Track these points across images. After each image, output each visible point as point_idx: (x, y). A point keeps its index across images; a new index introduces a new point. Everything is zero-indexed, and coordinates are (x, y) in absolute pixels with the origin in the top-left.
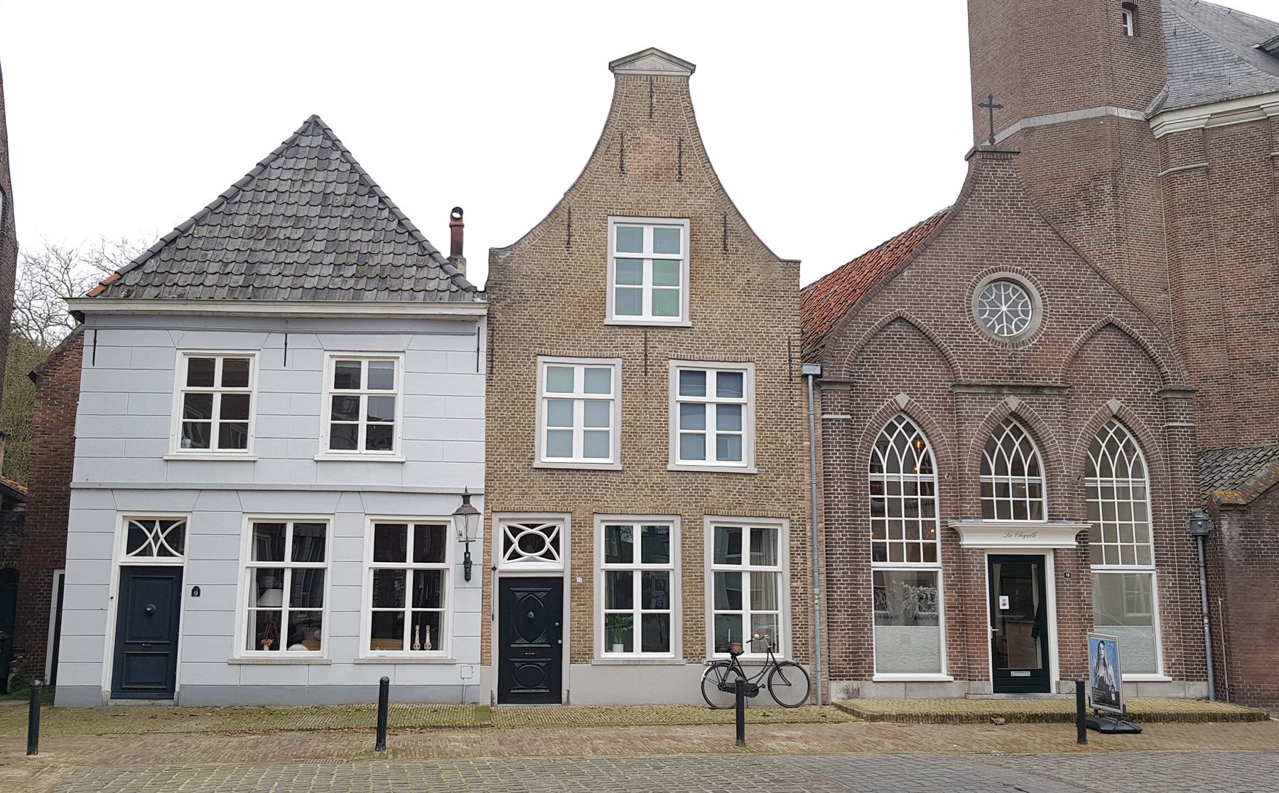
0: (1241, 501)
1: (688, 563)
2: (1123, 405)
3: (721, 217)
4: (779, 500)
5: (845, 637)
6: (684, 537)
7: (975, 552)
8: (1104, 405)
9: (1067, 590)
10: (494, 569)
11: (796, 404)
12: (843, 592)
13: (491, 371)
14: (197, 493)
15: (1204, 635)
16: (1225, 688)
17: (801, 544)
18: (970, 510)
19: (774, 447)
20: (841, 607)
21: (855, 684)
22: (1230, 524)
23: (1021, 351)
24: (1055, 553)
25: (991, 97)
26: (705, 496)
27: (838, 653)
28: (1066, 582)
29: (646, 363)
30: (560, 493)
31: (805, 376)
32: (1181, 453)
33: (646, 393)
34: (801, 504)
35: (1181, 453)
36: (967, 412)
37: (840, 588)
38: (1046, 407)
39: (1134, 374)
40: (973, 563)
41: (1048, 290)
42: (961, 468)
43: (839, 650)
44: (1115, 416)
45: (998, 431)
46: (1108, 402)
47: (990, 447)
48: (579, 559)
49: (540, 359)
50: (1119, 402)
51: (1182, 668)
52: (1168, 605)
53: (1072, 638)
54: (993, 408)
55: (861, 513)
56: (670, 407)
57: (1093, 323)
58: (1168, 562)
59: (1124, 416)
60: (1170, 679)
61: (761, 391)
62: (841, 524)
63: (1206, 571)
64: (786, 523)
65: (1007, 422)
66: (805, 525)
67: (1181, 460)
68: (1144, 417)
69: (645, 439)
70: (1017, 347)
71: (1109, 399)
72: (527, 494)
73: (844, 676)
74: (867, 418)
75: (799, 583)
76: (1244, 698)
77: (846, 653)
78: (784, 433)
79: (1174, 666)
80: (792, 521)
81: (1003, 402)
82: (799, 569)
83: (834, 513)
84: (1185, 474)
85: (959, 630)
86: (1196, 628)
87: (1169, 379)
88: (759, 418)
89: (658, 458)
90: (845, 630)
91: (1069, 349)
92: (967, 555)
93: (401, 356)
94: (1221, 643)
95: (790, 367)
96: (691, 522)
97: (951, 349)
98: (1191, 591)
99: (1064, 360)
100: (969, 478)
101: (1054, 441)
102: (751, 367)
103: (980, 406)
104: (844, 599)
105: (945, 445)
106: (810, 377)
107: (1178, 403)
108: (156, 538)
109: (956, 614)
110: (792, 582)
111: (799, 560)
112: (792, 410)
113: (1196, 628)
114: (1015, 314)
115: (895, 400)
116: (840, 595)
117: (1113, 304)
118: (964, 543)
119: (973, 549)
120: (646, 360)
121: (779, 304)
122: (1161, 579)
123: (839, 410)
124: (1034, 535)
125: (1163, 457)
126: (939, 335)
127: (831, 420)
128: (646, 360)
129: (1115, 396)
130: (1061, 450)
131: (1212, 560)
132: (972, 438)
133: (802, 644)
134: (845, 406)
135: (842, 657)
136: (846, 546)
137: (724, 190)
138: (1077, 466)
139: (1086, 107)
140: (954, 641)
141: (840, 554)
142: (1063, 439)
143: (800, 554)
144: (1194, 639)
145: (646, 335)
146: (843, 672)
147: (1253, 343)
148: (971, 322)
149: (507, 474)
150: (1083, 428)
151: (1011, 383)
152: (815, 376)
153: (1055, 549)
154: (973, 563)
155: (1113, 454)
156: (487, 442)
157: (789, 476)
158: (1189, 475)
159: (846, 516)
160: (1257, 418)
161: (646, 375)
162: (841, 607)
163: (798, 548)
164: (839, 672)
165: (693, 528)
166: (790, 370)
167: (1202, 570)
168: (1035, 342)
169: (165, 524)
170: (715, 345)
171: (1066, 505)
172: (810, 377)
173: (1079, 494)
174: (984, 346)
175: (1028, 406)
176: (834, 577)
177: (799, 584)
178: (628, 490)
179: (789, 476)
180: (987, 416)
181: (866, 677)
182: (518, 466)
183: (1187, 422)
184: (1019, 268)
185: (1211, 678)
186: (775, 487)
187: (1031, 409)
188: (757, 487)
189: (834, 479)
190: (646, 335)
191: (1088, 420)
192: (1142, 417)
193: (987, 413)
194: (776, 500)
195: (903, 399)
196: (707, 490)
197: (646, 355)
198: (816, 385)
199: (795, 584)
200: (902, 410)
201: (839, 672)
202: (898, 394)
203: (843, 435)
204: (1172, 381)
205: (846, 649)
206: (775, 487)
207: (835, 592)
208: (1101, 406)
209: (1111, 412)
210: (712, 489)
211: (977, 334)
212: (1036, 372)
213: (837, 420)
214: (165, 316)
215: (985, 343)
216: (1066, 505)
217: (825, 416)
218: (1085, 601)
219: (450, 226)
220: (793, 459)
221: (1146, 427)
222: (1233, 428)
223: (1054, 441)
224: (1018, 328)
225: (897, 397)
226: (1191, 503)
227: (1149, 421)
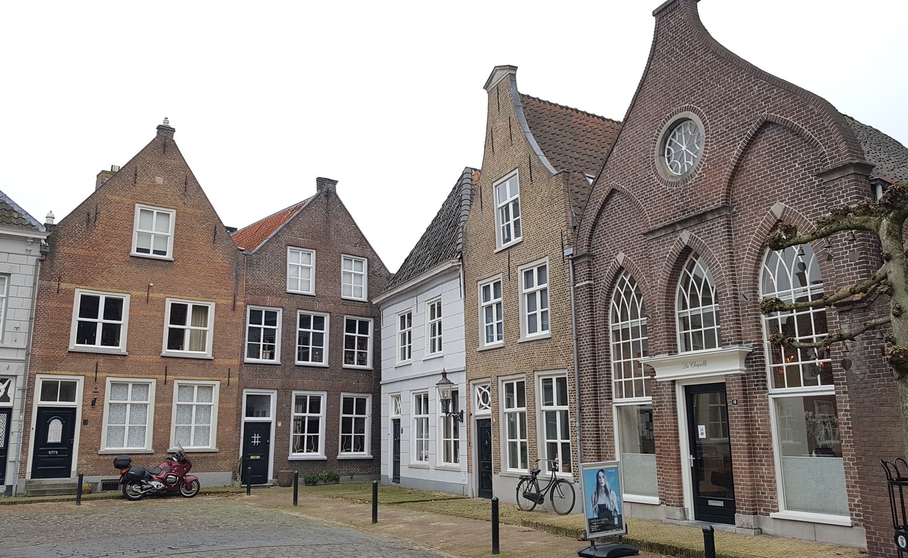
2: (787, 206)
7: (664, 385)
8: (769, 212)
14: (428, 378)
18: (660, 346)
23: (690, 185)
28: (735, 410)
35: (842, 245)
38: (710, 233)
39: (797, 166)
40: (663, 395)
41: (709, 115)
50: (783, 204)
53: (742, 468)
54: (672, 247)
57: (748, 129)
68: (809, 213)
70: (687, 182)
71: (772, 204)
79: (857, 509)
84: (848, 270)
87: (826, 160)
91: (727, 167)
99: (723, 180)
103: (663, 248)
117: (767, 100)
119: (663, 382)
126: (635, 194)
129: (779, 199)
130: (724, 272)
132: (658, 279)
138: (746, 285)
142: (726, 261)
150: (750, 244)
151: (684, 217)
154: (663, 395)
158: (852, 269)
168: (700, 171)
171: (731, 328)
173: (749, 315)
174: (664, 190)
175: (696, 236)
184: (687, 105)
187: (700, 238)
191: (753, 233)
192: (807, 213)
195: (621, 257)
202: (618, 254)
204: (829, 161)
207: (585, 425)
208: (765, 214)
209: (775, 217)
212: (702, 201)
215: (664, 188)
218: (759, 429)
221: (811, 223)
223: (719, 265)
225: (618, 257)
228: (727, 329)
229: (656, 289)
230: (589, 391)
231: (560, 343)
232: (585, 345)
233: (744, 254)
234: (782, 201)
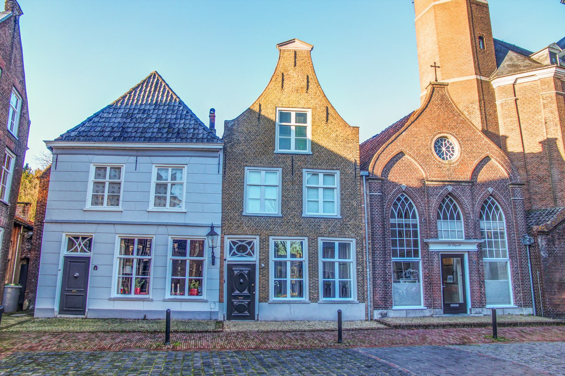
0: (546, 230)
1: (311, 258)
3: (325, 109)
4: (351, 230)
5: (380, 290)
6: (309, 246)
9: (474, 269)
10: (225, 260)
11: (358, 188)
12: (380, 270)
13: (224, 173)
15: (530, 288)
16: (541, 310)
19: (349, 207)
20: (379, 277)
21: (385, 311)
22: (541, 240)
23: (452, 167)
24: (468, 253)
25: (435, 63)
26: (319, 228)
27: (378, 297)
28: (474, 265)
29: (292, 170)
30: (254, 227)
31: (362, 176)
32: (518, 210)
33: (292, 183)
34: (361, 232)
35: (518, 210)
36: (431, 192)
37: (378, 269)
40: (435, 257)
42: (429, 216)
43: (378, 297)
44: (491, 195)
45: (443, 201)
46: (488, 189)
47: (440, 208)
48: (263, 256)
49: (246, 168)
51: (522, 302)
52: (515, 275)
53: (477, 289)
55: (387, 236)
56: (303, 189)
57: (481, 155)
58: (514, 256)
59: (494, 195)
60: (517, 307)
61: (343, 182)
62: (378, 241)
63: (531, 260)
64: (354, 240)
65: (447, 197)
66: (362, 241)
67: (519, 213)
69: (292, 203)
72: (240, 227)
73: (380, 308)
76: (550, 315)
80: (357, 239)
81: (445, 188)
82: (360, 260)
83: (376, 236)
84: (520, 219)
85: (429, 287)
86: (527, 285)
88: (342, 194)
89: (298, 212)
90: (380, 287)
92: (432, 254)
93: (186, 166)
94: (539, 291)
95: (355, 172)
97: (424, 165)
98: (524, 269)
100: (433, 221)
101: (467, 205)
102: (338, 172)
104: (380, 274)
105: (422, 206)
106: (364, 176)
107: (516, 189)
108: (80, 245)
109: (428, 280)
110: (357, 266)
111: (360, 257)
112: (356, 191)
113: (527, 285)
114: (449, 151)
115: (400, 187)
116: (378, 272)
118: (431, 249)
120: (292, 168)
121: (350, 145)
122: (512, 264)
123: (377, 191)
125: (511, 212)
127: (374, 195)
128: (292, 168)
131: (533, 255)
133: (362, 294)
134: (379, 189)
135: (379, 299)
136: (381, 250)
139: (466, 75)
140: (427, 291)
141: (378, 254)
143: (360, 254)
144: (526, 289)
145: (292, 158)
147: (537, 168)
148: (432, 154)
149: (231, 218)
152: (366, 176)
153: (468, 251)
154: (435, 257)
155: (490, 211)
156: (222, 204)
157: (355, 220)
159: (381, 237)
160: (540, 199)
161: (292, 175)
162: (379, 277)
163: (360, 251)
164: (378, 306)
165: (313, 242)
166: (355, 174)
167: (529, 260)
168: (458, 163)
169: (84, 238)
170: (322, 162)
171: (473, 232)
172: (364, 176)
176: (376, 264)
177: (360, 267)
178: (284, 225)
179: (355, 220)
180: (439, 194)
181: (390, 308)
182: (236, 215)
183: (520, 197)
184: (450, 132)
186: (349, 225)
188: (341, 224)
189: (375, 221)
190: (292, 158)
192: (502, 195)
193: (439, 193)
194: (350, 230)
196: (320, 226)
197: (292, 167)
199: (358, 267)
200: (403, 192)
201: (378, 306)
203: (379, 202)
205: (381, 296)
206: (349, 225)
207: (376, 271)
208: (485, 190)
211: (434, 159)
213: (376, 195)
214: (84, 149)
216: (473, 232)
217: (371, 194)
219: (210, 116)
220: (357, 212)
221: (504, 199)
222: (530, 203)
223: (467, 205)
224: (450, 157)
226: (523, 232)
227: (505, 197)
228: (471, 232)
229: (432, 208)
231: (349, 223)
233: (476, 203)
234: (492, 188)
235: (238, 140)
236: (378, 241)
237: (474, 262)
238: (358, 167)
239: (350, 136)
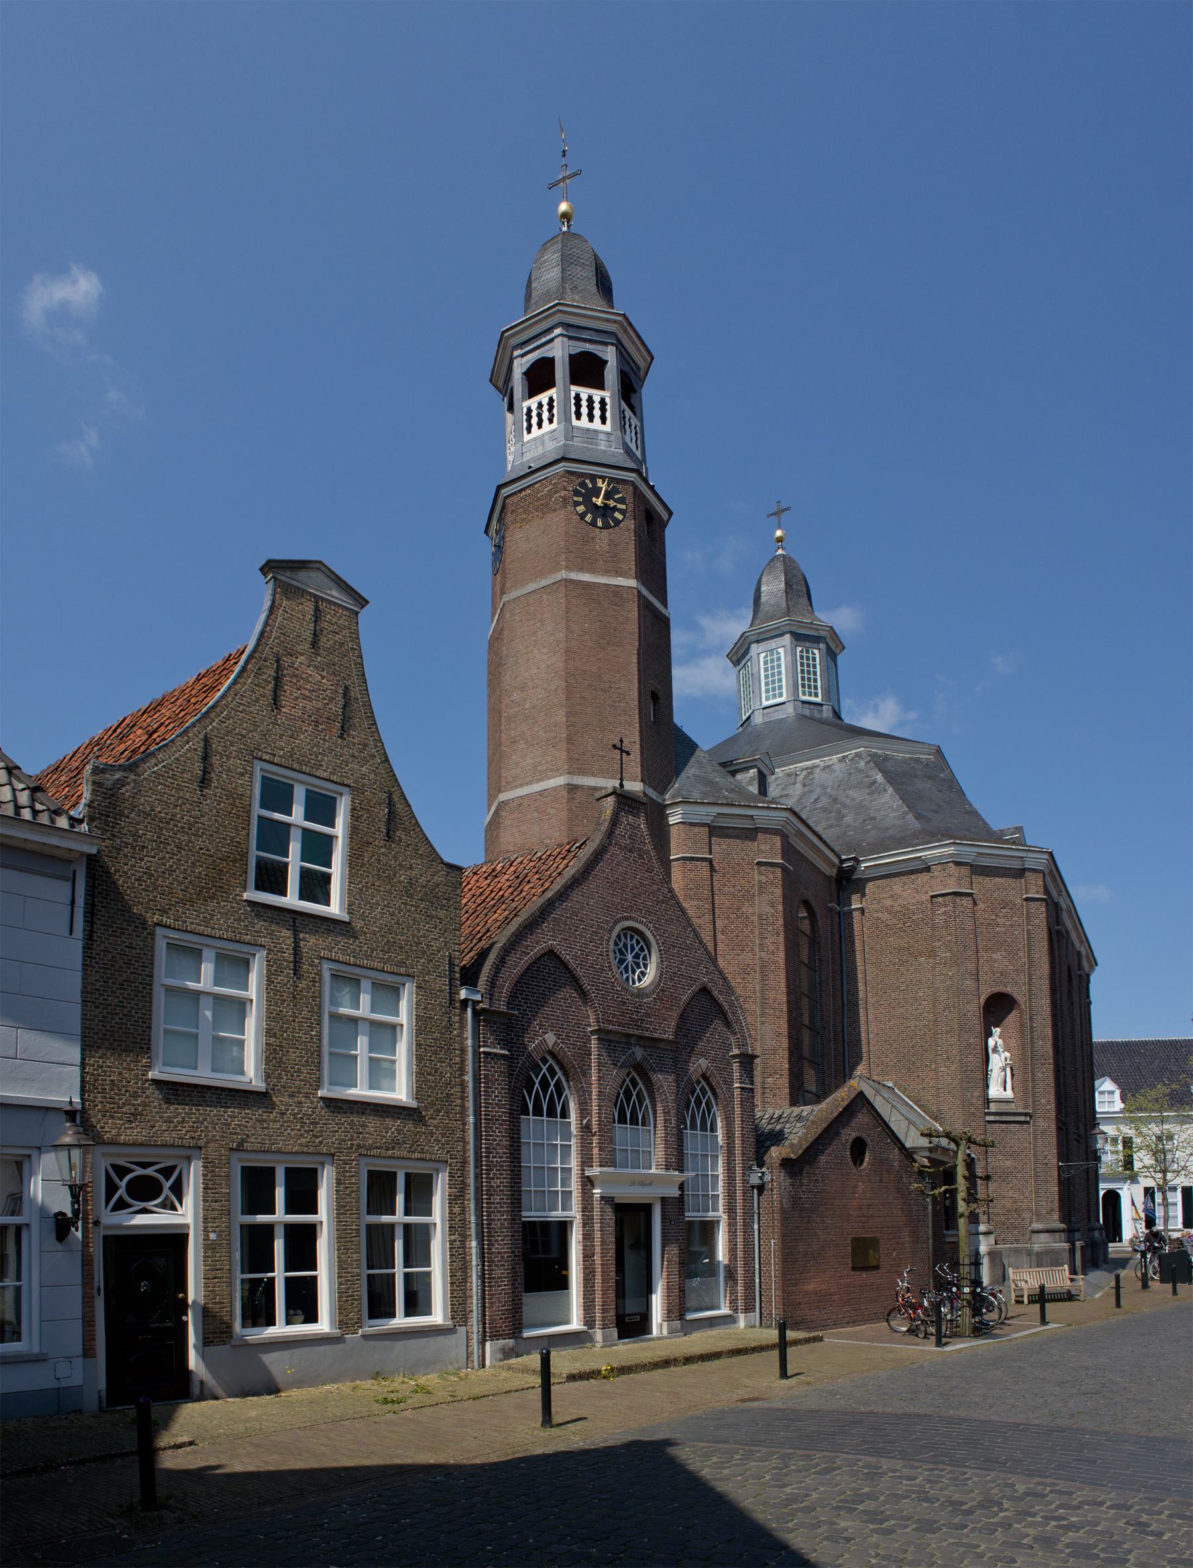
9: (672, 1236)
17: (459, 1192)
24: (662, 1202)
62: (499, 1170)
63: (759, 1217)
69: (293, 1055)
73: (500, 1335)
74: (519, 1055)
75: (457, 1236)
77: (502, 1310)
78: (444, 1065)
88: (418, 1045)
96: (346, 1164)
116: (498, 1249)
124: (650, 1184)
131: (766, 1208)
135: (498, 1315)
136: (503, 1195)
137: (389, 764)
141: (498, 1203)
143: (457, 1203)
145: (294, 922)
146: (499, 1331)
153: (662, 1198)
159: (504, 1162)
165: (347, 1172)
185: (758, 1310)
190: (294, 922)
198: (476, 1013)
210: (369, 1124)
230: (503, 1199)
232: (497, 1136)
235: (136, 836)
236: (499, 1170)
237: (673, 1222)
238: (458, 975)
239: (442, 888)
